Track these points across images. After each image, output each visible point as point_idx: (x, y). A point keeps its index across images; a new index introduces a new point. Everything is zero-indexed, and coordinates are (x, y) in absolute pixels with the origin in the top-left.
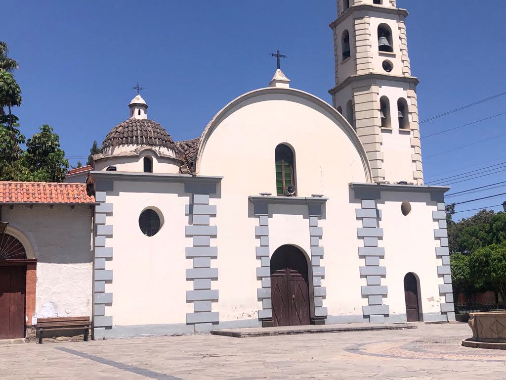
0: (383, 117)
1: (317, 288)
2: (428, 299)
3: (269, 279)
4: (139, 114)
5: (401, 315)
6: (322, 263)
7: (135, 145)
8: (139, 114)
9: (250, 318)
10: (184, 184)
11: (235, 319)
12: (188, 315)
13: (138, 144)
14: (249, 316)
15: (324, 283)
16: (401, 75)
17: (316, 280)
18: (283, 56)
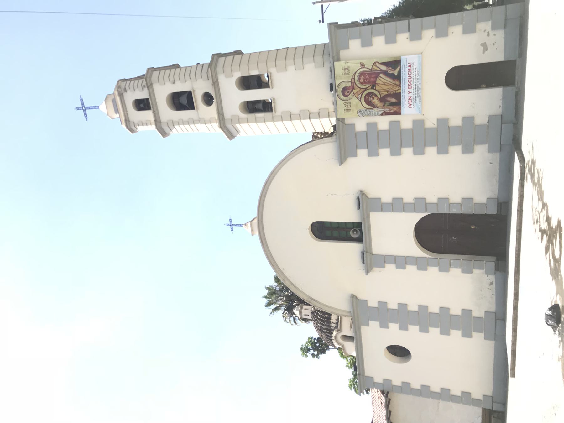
0: (260, 106)
1: (463, 209)
2: (483, 53)
3: (452, 261)
4: (308, 315)
5: (504, 97)
6: (432, 198)
7: (333, 341)
8: (308, 315)
9: (494, 283)
10: (361, 326)
11: (494, 297)
12: (485, 338)
13: (332, 340)
14: (491, 283)
15: (456, 198)
16: (211, 81)
17: (454, 210)
18: (231, 222)
